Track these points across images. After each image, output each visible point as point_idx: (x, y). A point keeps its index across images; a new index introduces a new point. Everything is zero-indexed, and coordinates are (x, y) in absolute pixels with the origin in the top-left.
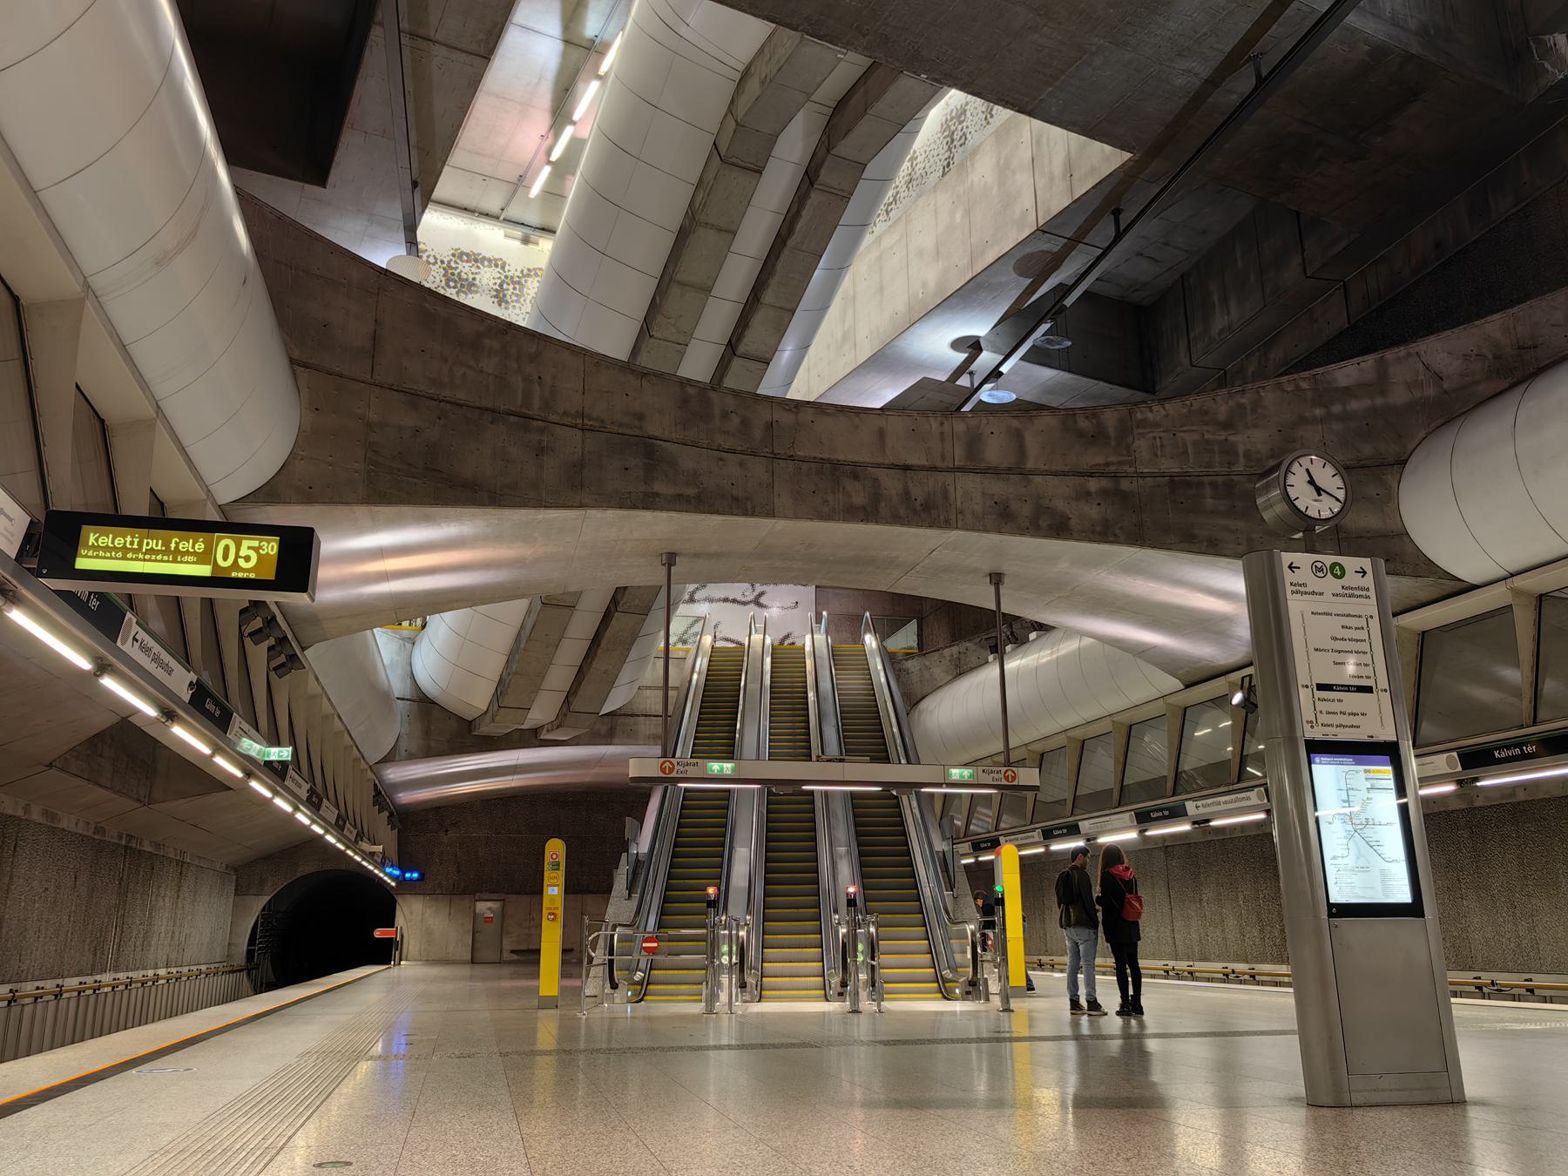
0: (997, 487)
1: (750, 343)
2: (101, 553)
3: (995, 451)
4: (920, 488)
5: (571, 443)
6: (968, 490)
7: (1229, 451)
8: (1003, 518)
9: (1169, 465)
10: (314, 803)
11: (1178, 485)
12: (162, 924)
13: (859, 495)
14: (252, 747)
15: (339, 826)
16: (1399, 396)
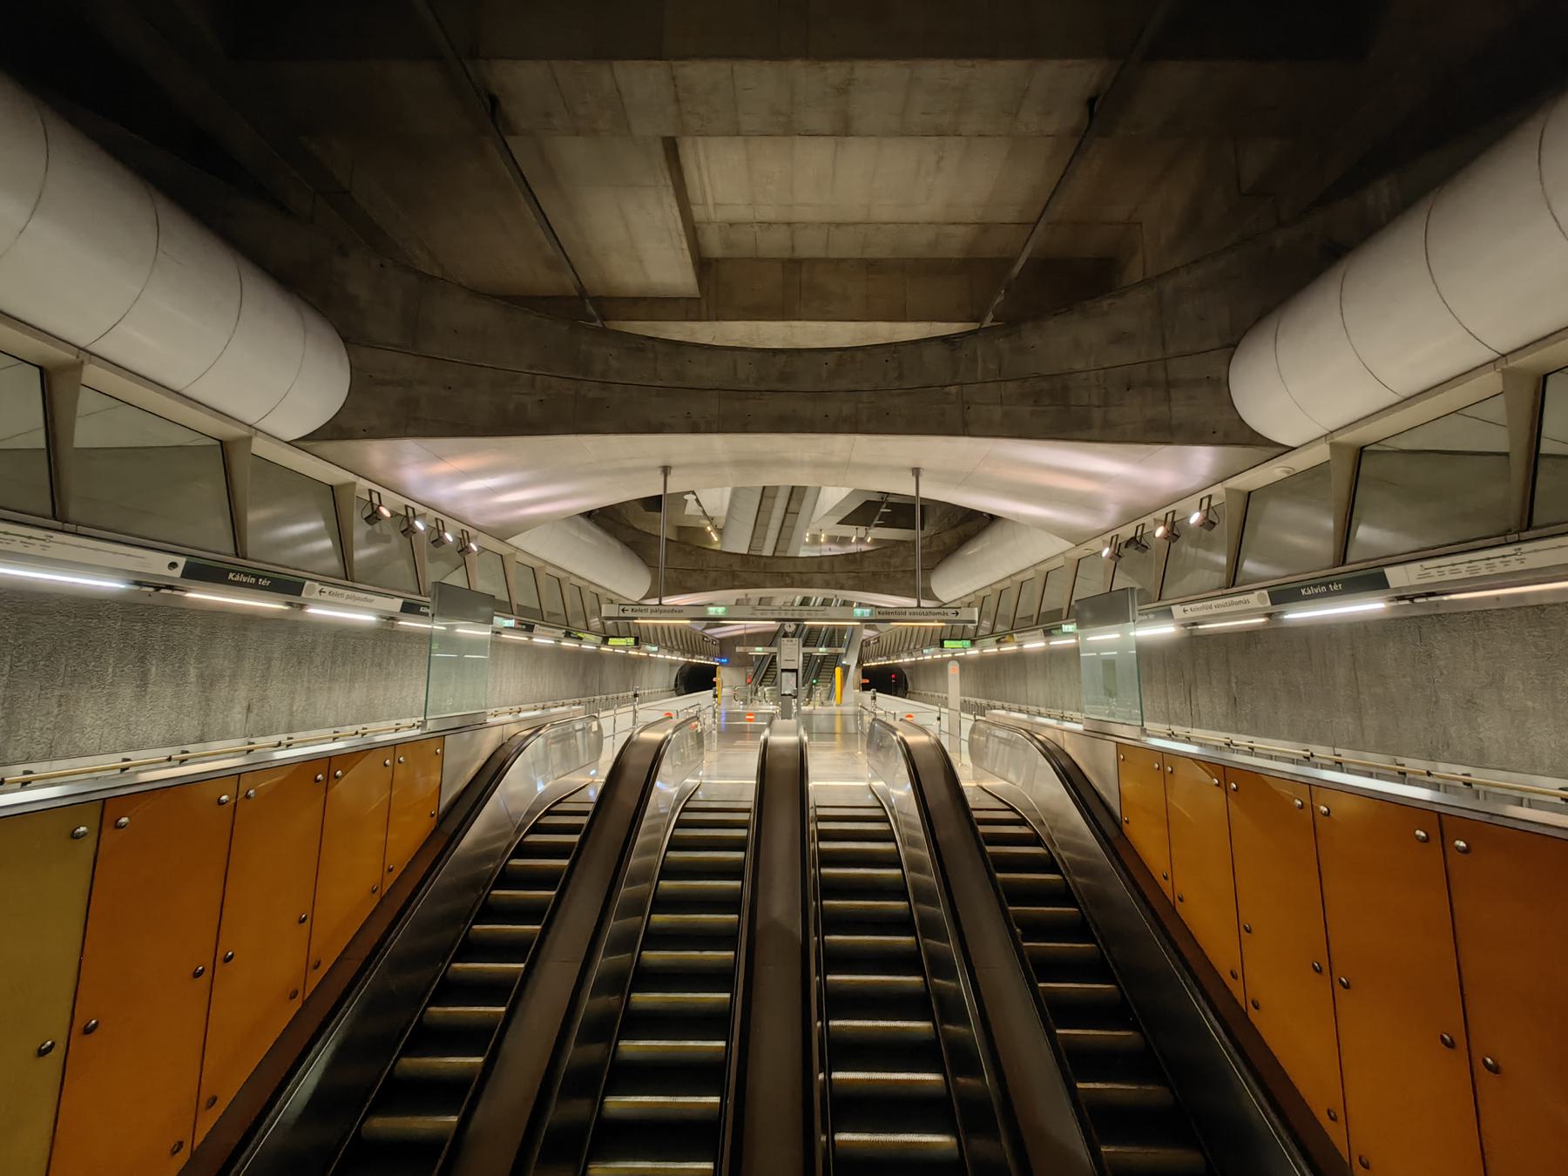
0: (827, 577)
1: (793, 507)
2: (612, 641)
3: (826, 567)
4: (805, 578)
5: (713, 575)
6: (818, 578)
7: (889, 564)
8: (827, 585)
9: (872, 569)
10: (671, 650)
11: (874, 574)
12: (645, 677)
13: (788, 581)
14: (649, 648)
15: (683, 655)
16: (934, 548)
